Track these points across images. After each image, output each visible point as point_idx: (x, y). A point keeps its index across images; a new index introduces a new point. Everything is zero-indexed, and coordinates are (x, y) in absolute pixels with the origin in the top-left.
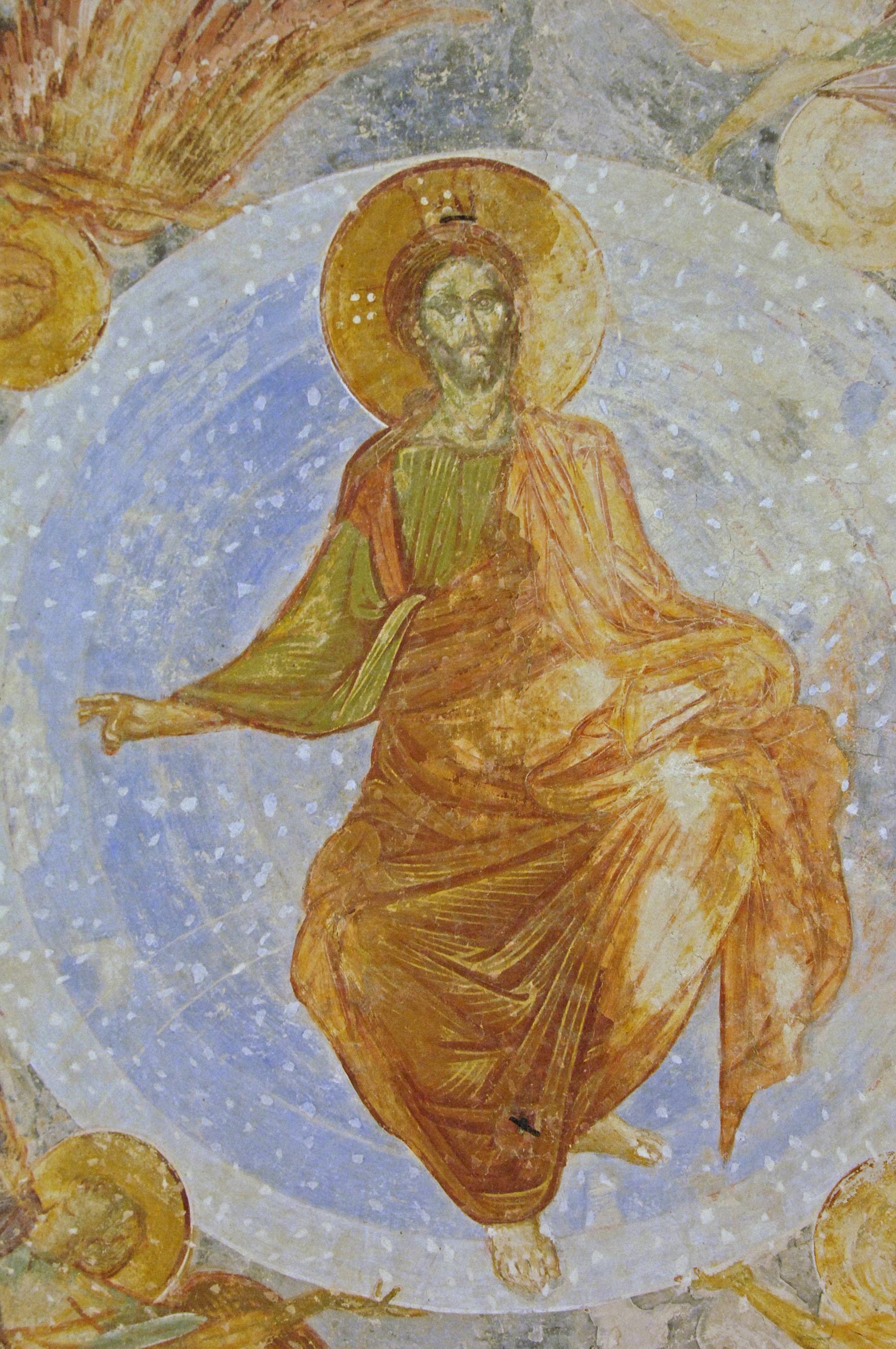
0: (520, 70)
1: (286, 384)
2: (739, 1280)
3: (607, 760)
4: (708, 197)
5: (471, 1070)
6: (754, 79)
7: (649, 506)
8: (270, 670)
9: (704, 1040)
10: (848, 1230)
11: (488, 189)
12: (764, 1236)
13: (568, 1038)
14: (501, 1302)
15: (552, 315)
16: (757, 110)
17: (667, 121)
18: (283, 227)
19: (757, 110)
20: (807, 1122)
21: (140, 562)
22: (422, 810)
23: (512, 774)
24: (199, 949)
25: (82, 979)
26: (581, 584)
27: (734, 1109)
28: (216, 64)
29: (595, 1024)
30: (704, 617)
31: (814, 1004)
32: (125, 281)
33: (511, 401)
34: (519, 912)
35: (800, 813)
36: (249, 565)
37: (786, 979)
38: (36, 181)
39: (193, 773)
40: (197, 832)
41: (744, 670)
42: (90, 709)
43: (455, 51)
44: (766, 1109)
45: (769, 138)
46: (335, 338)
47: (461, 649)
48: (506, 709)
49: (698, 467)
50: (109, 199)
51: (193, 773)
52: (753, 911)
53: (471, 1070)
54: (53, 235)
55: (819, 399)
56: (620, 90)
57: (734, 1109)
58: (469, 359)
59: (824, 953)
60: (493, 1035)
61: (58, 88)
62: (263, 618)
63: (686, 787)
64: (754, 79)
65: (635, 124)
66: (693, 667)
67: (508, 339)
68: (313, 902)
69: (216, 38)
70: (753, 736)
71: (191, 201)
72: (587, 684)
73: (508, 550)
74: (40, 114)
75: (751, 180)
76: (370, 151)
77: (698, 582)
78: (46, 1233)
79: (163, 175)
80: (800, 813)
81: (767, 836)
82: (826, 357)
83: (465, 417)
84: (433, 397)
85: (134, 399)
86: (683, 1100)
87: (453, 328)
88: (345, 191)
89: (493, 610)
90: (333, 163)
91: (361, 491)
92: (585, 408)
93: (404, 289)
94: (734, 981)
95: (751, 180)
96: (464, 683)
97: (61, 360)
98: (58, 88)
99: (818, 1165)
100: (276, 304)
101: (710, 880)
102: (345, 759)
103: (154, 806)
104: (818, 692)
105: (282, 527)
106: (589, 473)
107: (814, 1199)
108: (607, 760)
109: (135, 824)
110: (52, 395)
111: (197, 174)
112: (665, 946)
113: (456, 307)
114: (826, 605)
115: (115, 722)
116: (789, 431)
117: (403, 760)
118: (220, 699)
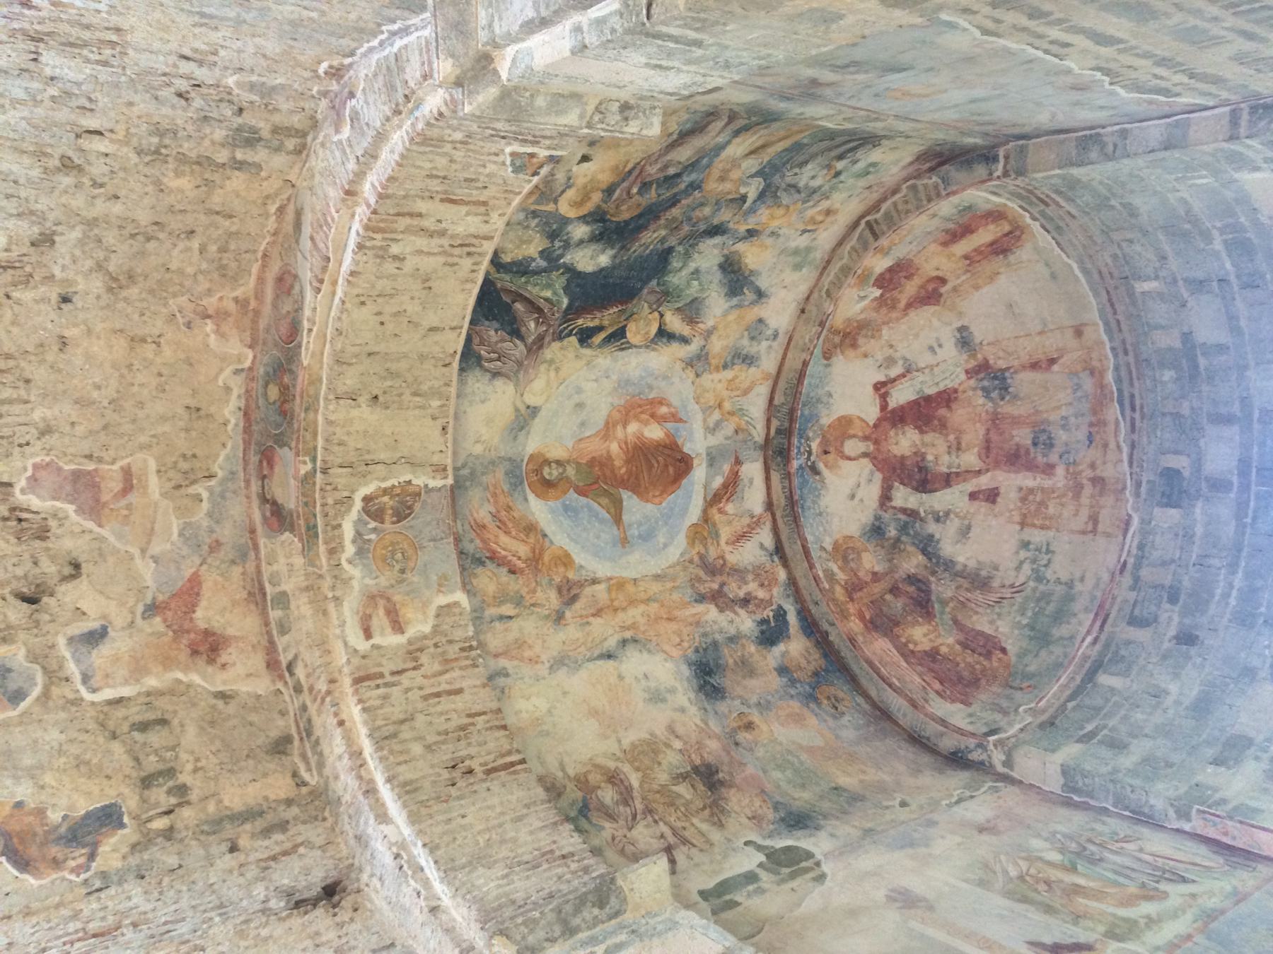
0: (510, 459)
1: (566, 508)
2: (705, 420)
3: (626, 443)
4: (537, 420)
5: (671, 470)
6: (517, 410)
7: (587, 434)
8: (612, 510)
9: (669, 425)
10: (702, 400)
11: (531, 466)
12: (700, 416)
13: (667, 451)
14: (704, 465)
15: (557, 453)
16: (522, 408)
17: (522, 428)
18: (538, 509)
19: (522, 408)
20: (685, 407)
21: (598, 537)
22: (632, 479)
23: (628, 461)
24: (657, 522)
25: (665, 546)
26: (595, 448)
27: (681, 420)
28: (510, 525)
29: (665, 446)
30: (607, 423)
31: (669, 405)
32: (551, 542)
33: (568, 462)
34: (648, 461)
35: (640, 406)
36: (596, 516)
37: (664, 410)
38: (537, 561)
39: (630, 525)
40: (640, 524)
41: (617, 416)
42: (624, 547)
43: (506, 474)
44: (682, 415)
45: (528, 407)
46: (557, 499)
47: (608, 473)
48: (617, 463)
49: (583, 424)
50: (538, 546)
51: (630, 525)
52: (653, 416)
53: (671, 470)
54: (546, 558)
55: (576, 399)
56: (515, 438)
57: (681, 420)
58: (561, 470)
59: (661, 402)
60: (666, 466)
61: (519, 558)
62: (604, 512)
63: (633, 427)
64: (517, 410)
65: (522, 435)
66: (614, 426)
67: (558, 463)
68: (647, 501)
69: (505, 524)
70: (627, 415)
71: (536, 529)
72: (614, 447)
73: (592, 462)
74: (525, 561)
75: (534, 411)
76: (524, 491)
77: (601, 424)
78: (703, 551)
79: (532, 535)
80: (640, 406)
81: (642, 413)
82: (569, 398)
83: (571, 471)
84: (567, 477)
85: (572, 540)
86: (677, 430)
87: (555, 473)
88: (531, 497)
89: (602, 465)
90: (526, 500)
91: (582, 492)
92: (570, 445)
93: (548, 484)
94: (661, 420)
95: (534, 411)
96: (613, 471)
97: (568, 555)
98: (519, 558)
99: (694, 407)
100: (552, 511)
101: (646, 423)
102: (626, 495)
103: (636, 533)
104: (622, 402)
105: (590, 509)
106: (582, 446)
107: (697, 407)
108: (626, 443)
109: (640, 536)
110: (574, 557)
111: (531, 528)
112: (655, 433)
113: (551, 473)
114: (610, 399)
115: (624, 541)
116: (580, 406)
117: (624, 483)
118: (618, 520)
